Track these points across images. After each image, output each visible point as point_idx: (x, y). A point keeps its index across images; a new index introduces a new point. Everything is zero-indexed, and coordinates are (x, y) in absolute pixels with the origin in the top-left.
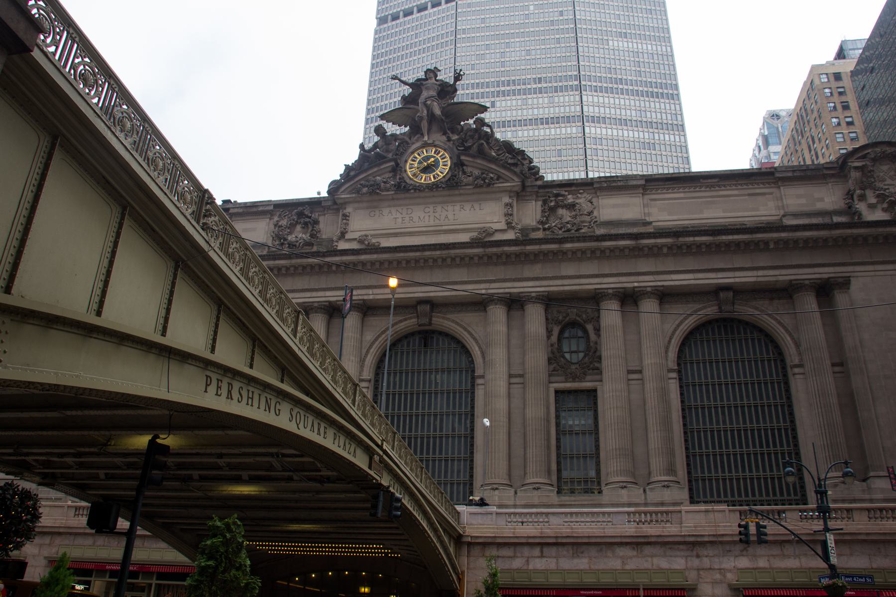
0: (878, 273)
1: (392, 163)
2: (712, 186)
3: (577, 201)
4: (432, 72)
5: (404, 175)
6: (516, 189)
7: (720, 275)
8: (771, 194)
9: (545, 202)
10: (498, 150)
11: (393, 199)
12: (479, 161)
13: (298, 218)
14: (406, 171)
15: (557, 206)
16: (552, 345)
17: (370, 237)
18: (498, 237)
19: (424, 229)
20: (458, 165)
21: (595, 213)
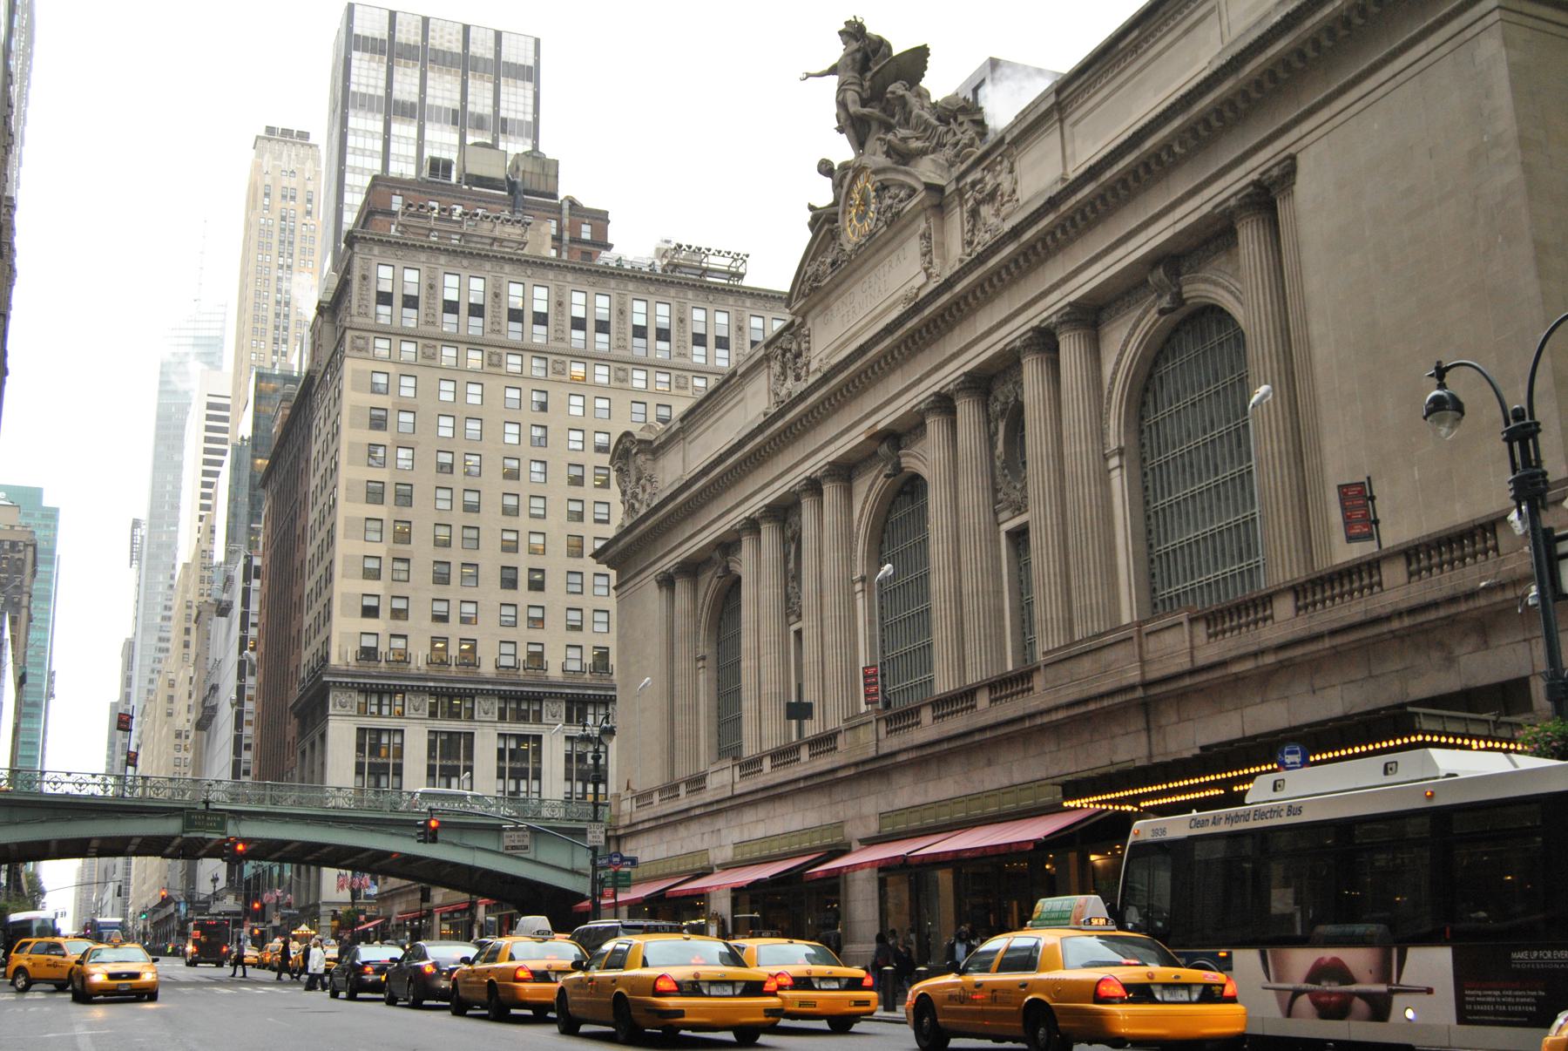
6: (927, 203)
15: (979, 203)
18: (922, 294)
21: (1018, 194)
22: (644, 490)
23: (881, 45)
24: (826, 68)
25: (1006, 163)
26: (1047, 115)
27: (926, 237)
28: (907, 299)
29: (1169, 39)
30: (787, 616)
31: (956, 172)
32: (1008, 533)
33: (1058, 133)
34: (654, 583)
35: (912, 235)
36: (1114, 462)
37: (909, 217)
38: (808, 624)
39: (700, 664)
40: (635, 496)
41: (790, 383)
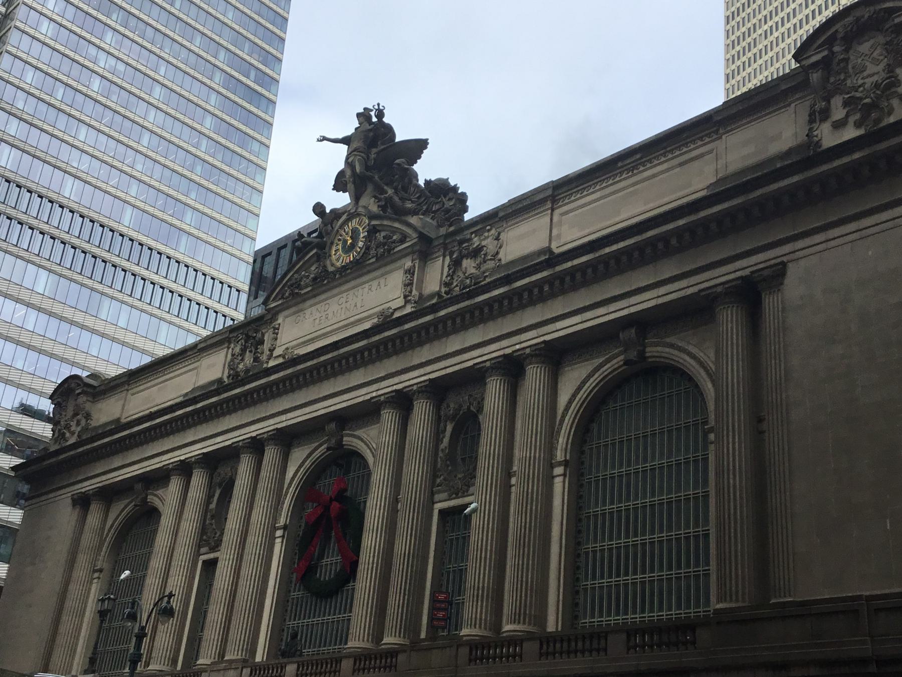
0: (833, 243)
1: (315, 251)
2: (633, 169)
3: (484, 243)
4: (364, 116)
5: (328, 262)
6: (418, 248)
7: (613, 307)
8: (710, 152)
9: (451, 255)
10: (419, 198)
11: (315, 296)
12: (385, 223)
13: (246, 342)
14: (330, 256)
15: (461, 257)
16: (442, 450)
17: (290, 351)
19: (335, 327)
20: (373, 231)
21: (501, 255)
22: (78, 424)
23: (389, 129)
24: (340, 137)
25: (493, 231)
26: (543, 201)
27: (410, 272)
28: (382, 313)
29: (665, 166)
30: (200, 547)
31: (443, 231)
32: (440, 511)
33: (548, 219)
34: (69, 501)
35: (400, 268)
36: (559, 470)
37: (397, 256)
38: (225, 557)
39: (96, 575)
40: (68, 427)
41: (249, 359)
